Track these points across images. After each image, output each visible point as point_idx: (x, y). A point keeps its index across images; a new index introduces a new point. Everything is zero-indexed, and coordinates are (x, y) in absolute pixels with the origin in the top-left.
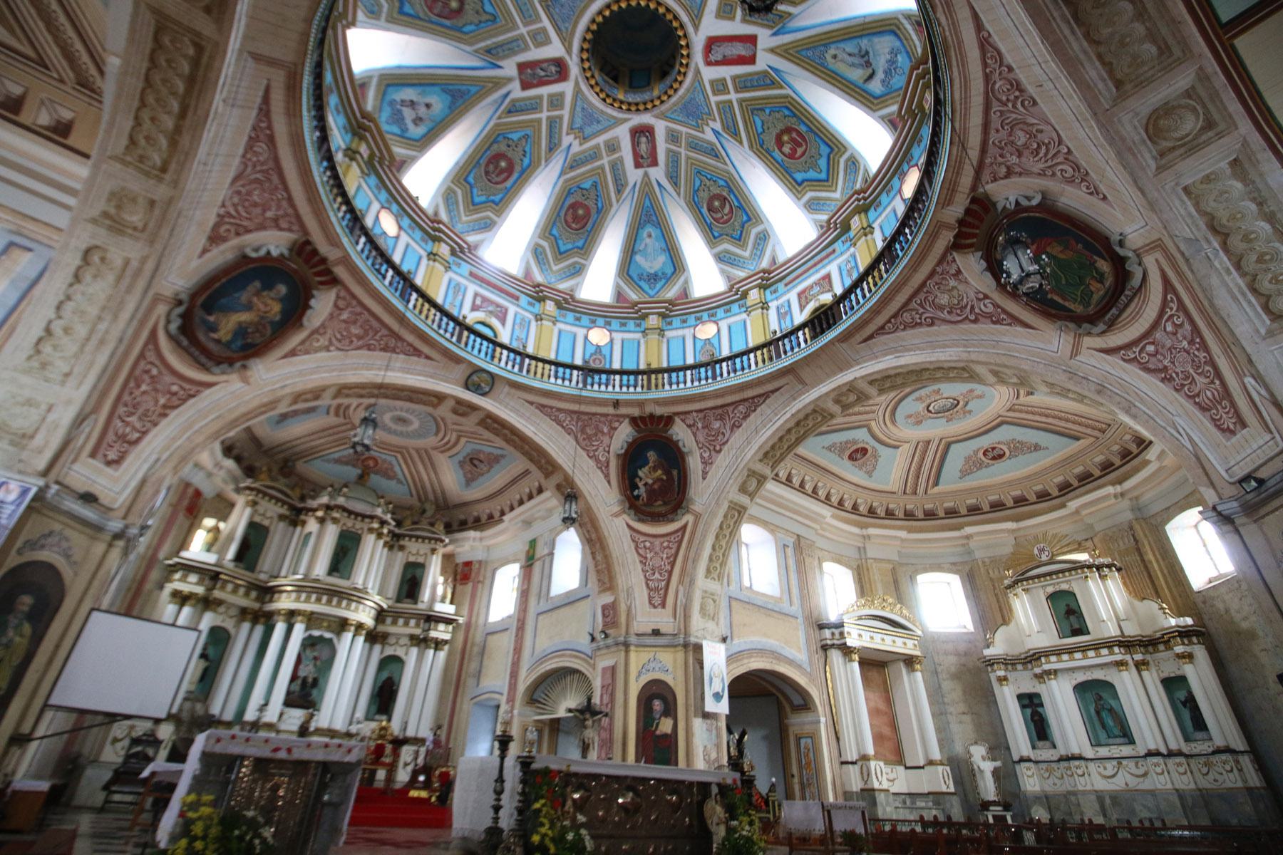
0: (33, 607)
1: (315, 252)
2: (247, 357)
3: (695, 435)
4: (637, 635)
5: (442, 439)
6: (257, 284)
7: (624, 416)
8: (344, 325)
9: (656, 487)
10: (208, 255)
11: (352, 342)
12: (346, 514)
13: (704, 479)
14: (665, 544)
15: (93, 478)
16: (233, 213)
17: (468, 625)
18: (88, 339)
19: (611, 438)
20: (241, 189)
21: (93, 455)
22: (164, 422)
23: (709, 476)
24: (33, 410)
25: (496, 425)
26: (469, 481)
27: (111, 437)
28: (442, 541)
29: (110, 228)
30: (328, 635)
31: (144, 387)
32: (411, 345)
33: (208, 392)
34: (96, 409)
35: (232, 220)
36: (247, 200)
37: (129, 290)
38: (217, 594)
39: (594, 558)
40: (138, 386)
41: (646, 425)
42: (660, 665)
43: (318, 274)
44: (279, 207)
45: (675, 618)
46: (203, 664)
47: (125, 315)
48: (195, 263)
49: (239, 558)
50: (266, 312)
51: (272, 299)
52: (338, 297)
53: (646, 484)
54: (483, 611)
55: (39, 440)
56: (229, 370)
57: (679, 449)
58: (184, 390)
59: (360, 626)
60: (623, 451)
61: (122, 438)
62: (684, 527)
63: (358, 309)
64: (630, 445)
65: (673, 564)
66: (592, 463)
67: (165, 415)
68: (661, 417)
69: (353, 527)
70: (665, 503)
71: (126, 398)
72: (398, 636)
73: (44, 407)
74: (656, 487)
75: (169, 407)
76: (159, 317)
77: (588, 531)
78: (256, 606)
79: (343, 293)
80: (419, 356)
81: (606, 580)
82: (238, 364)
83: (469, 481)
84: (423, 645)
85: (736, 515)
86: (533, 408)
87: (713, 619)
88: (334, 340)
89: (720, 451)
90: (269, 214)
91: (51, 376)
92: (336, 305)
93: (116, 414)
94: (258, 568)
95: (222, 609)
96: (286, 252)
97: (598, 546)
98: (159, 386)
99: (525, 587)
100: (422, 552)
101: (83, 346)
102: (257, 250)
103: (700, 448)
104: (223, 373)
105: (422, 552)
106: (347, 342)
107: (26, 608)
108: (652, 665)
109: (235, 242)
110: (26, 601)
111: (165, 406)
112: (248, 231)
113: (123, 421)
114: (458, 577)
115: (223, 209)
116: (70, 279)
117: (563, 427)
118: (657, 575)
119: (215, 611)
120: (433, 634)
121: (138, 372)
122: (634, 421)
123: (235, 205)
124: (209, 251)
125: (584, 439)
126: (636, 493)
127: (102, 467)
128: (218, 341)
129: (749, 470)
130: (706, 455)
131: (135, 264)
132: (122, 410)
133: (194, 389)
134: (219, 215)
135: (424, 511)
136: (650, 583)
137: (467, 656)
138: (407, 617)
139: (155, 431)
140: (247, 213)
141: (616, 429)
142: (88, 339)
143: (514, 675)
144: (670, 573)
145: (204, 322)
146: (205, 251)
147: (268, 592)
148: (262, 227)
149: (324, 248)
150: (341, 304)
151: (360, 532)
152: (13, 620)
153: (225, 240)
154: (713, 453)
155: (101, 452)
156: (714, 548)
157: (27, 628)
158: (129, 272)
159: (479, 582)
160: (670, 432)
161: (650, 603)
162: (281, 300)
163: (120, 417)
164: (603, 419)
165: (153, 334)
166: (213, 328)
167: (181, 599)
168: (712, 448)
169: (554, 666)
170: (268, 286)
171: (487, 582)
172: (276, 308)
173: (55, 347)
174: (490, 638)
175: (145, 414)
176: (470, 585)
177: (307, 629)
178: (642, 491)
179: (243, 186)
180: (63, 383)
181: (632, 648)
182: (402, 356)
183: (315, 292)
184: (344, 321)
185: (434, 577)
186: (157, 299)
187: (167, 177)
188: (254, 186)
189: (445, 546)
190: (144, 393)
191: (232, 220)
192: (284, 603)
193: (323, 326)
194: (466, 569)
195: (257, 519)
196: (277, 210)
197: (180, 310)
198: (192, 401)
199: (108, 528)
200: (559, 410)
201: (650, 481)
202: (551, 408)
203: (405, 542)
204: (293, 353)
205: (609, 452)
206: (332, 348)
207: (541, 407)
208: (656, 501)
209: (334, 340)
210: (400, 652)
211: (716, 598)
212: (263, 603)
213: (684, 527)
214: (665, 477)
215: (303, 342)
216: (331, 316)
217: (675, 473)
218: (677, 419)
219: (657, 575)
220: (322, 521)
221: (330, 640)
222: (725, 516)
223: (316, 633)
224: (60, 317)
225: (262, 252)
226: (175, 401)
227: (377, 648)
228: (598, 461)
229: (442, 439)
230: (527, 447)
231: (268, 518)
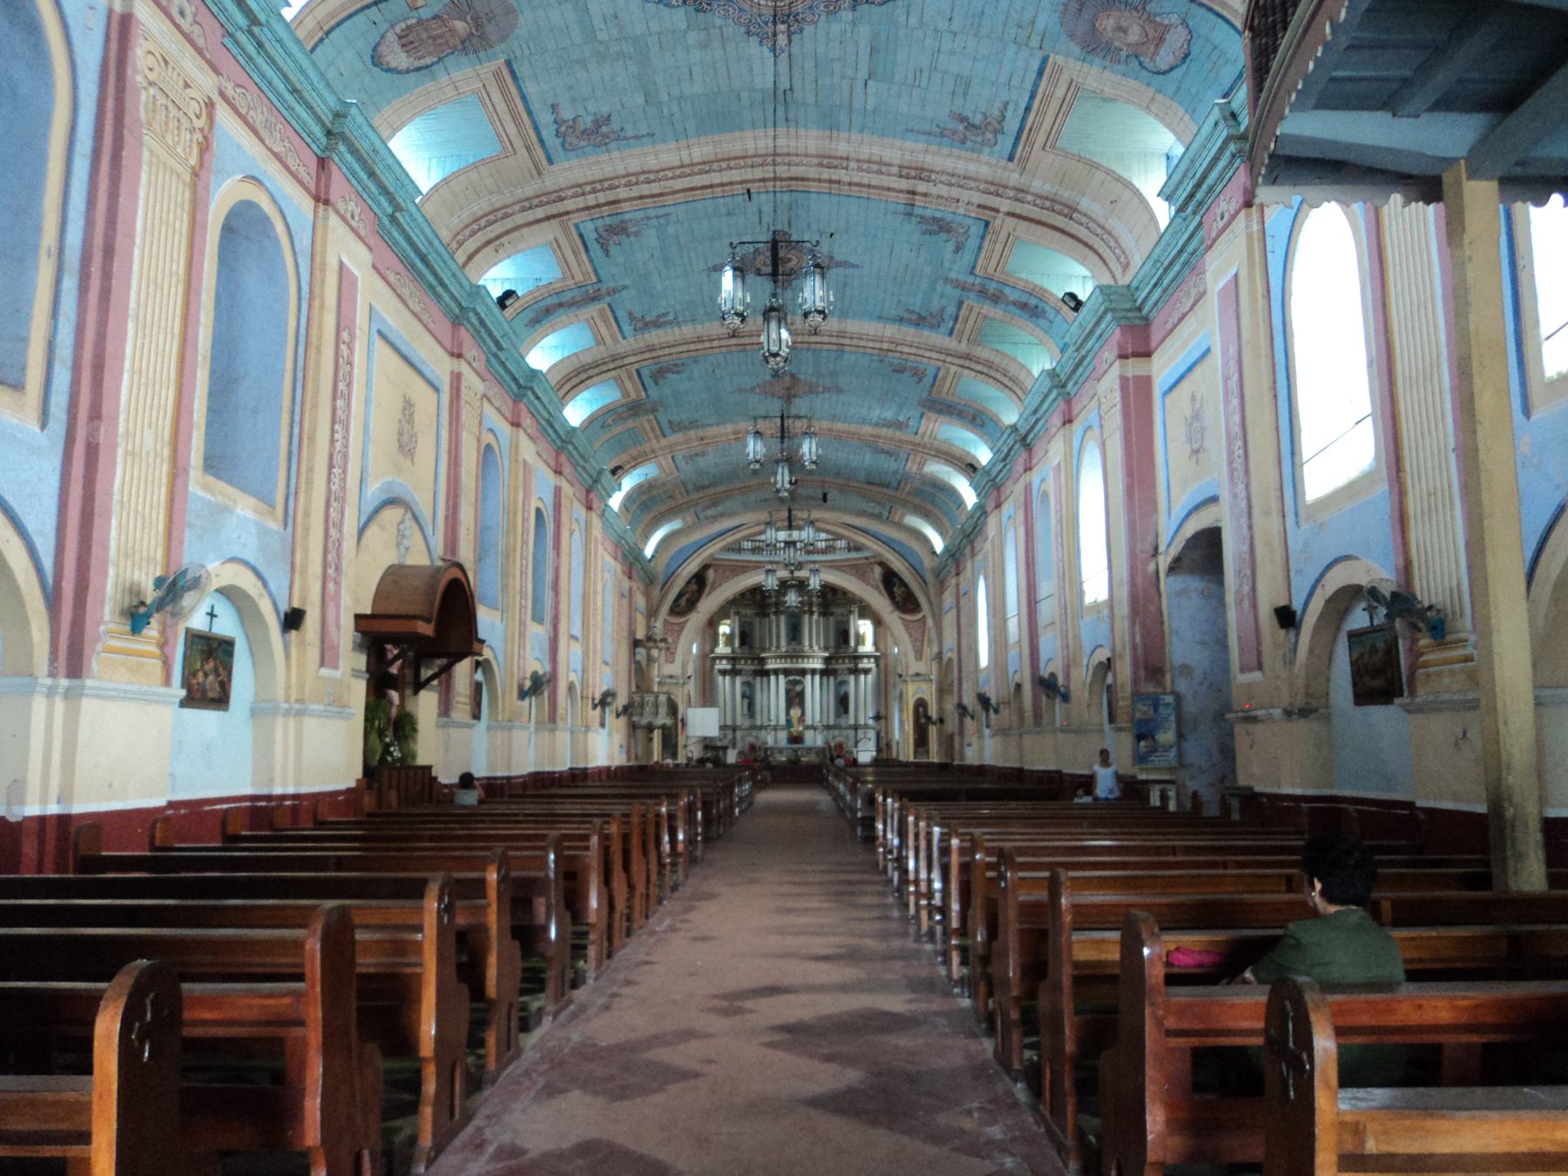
30: (798, 678)
38: (738, 667)
46: (746, 701)
49: (743, 642)
59: (813, 672)
66: (869, 588)
78: (759, 668)
120: (861, 666)
138: (844, 658)
147: (762, 661)
167: (724, 673)
178: (898, 599)
192: (771, 666)
210: (845, 678)
220: (776, 613)
223: (792, 678)
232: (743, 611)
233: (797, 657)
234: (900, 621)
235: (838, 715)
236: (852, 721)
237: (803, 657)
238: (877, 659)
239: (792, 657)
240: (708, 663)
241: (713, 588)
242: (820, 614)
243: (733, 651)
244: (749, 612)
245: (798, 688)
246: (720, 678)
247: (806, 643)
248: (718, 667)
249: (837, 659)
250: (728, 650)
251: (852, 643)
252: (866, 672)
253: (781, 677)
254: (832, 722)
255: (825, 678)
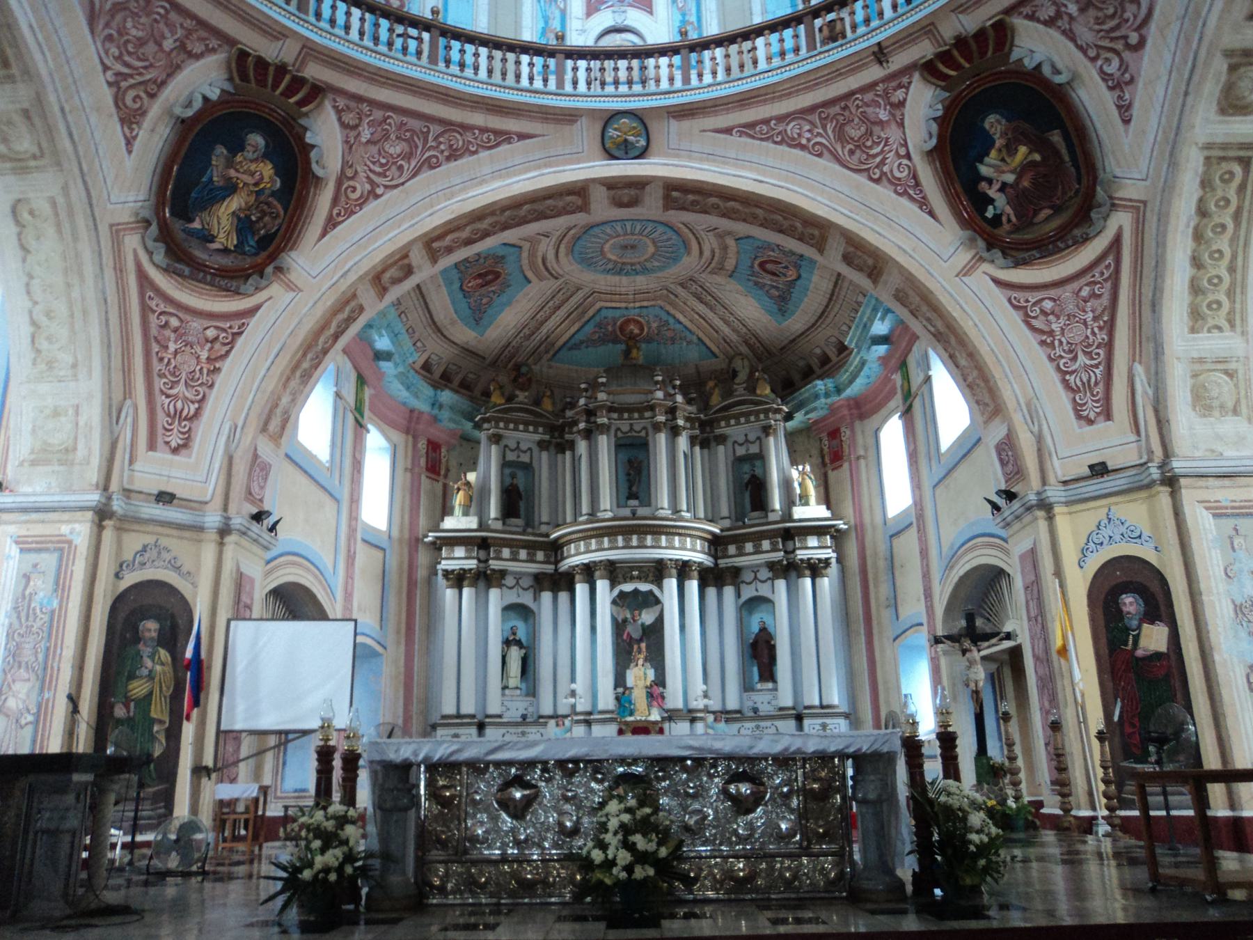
0: (161, 632)
1: (261, 63)
2: (272, 258)
3: (1070, 35)
4: (1065, 483)
5: (701, 253)
6: (220, 150)
7: (908, 70)
8: (374, 149)
9: (1026, 183)
10: (137, 144)
11: (401, 168)
12: (615, 415)
13: (1127, 122)
14: (1085, 292)
15: (166, 473)
16: (126, 70)
17: (859, 528)
18: (72, 316)
19: (901, 125)
20: (107, 31)
21: (152, 446)
22: (220, 379)
23: (1135, 111)
24: (63, 419)
25: (691, 197)
26: (782, 301)
27: (162, 419)
28: (778, 411)
29: (15, 171)
30: (644, 587)
31: (172, 347)
32: (484, 130)
33: (253, 321)
34: (128, 392)
35: (132, 81)
36: (128, 41)
37: (75, 238)
38: (495, 564)
39: (957, 367)
40: (167, 347)
41: (958, 67)
42: (1123, 529)
43: (290, 92)
44: (171, 27)
45: (1138, 433)
46: (515, 654)
47: (89, 269)
48: (129, 163)
50: (256, 184)
51: (255, 160)
52: (339, 112)
53: (1004, 187)
54: (877, 502)
55: (81, 452)
56: (264, 282)
57: (1046, 83)
58: (224, 330)
59: (683, 570)
60: (934, 141)
61: (177, 415)
62: (1117, 242)
63: (378, 114)
64: (941, 121)
65: (1110, 327)
66: (884, 192)
67: (217, 370)
68: (981, 34)
69: (631, 429)
70: (1057, 210)
71: (157, 366)
72: (755, 569)
73: (71, 412)
74: (1026, 183)
75: (215, 361)
76: (135, 251)
77: (928, 320)
78: (549, 568)
79: (341, 103)
80: (509, 140)
81: (987, 400)
82: (269, 269)
83: (782, 301)
84: (793, 574)
85: (1237, 169)
86: (734, 139)
87: (1235, 412)
88: (372, 176)
89: (1142, 43)
90: (168, 44)
91: (62, 373)
92: (344, 125)
93: (157, 392)
94: (536, 523)
95: (509, 581)
96: (228, 87)
97: (953, 340)
98: (191, 339)
99: (912, 447)
100: (752, 437)
101: (72, 325)
102: (189, 104)
103: (1093, 60)
104: (258, 289)
105: (752, 437)
106: (394, 171)
107: (154, 634)
108: (1106, 532)
109: (155, 109)
110: (150, 627)
111: (208, 358)
112: (163, 84)
113: (168, 396)
114: (827, 460)
115: (109, 73)
116: (20, 253)
117: (803, 147)
118: (1082, 359)
119: (500, 586)
120: (801, 554)
121: (154, 331)
122: (929, 69)
123: (119, 58)
124: (135, 138)
125: (852, 152)
126: (990, 213)
127: (170, 457)
128: (225, 251)
129: (1229, 54)
130: (1113, 68)
131: (61, 200)
132: (159, 383)
133: (236, 324)
134: (110, 84)
135: (735, 374)
136: (1071, 378)
137: (871, 576)
138: (757, 538)
139: (213, 395)
140: (139, 59)
141: (902, 104)
142: (72, 316)
143: (928, 594)
144: (1109, 346)
145: (192, 233)
146: (129, 143)
147: (555, 549)
148: (173, 70)
149: (270, 51)
150: (349, 118)
151: (643, 434)
152: (145, 650)
153: (142, 112)
154: (1127, 55)
155: (160, 440)
156: (1196, 262)
157: (164, 654)
158: (63, 215)
159: (858, 458)
160: (1015, 56)
161: (1079, 417)
162: (266, 156)
163: (162, 392)
164: (869, 97)
165: (142, 277)
166: (206, 237)
167: (458, 579)
168: (1119, 46)
169: (968, 567)
170: (237, 147)
171: (872, 452)
172: (267, 170)
173: (49, 339)
174: (896, 541)
175: (191, 377)
176: (846, 465)
177: (612, 586)
179: (107, 25)
180: (75, 377)
181: (1057, 509)
182: (484, 154)
183: (303, 122)
184: (369, 142)
185: (781, 470)
186: (117, 232)
187: (15, 70)
188: (119, 17)
189: (789, 417)
190: (176, 353)
191: (132, 81)
192: (576, 557)
193: (346, 164)
194: (835, 442)
195: (511, 457)
196: (173, 33)
197: (154, 229)
198: (240, 341)
199: (206, 525)
200: (781, 119)
201: (1010, 178)
202: (766, 122)
203: (722, 429)
204: (331, 223)
205: (908, 156)
206: (379, 191)
207: (748, 129)
208: (1036, 213)
209: (372, 176)
210: (764, 590)
211: (1232, 366)
212: (557, 563)
213: (1117, 242)
214: (1037, 157)
215: (335, 201)
216: (349, 145)
217: (1056, 137)
218: (1018, 22)
219: (1082, 359)
220: (588, 434)
221: (651, 592)
222: (1206, 184)
223: (628, 587)
224: (36, 303)
225: (198, 104)
226: (220, 349)
227: (729, 591)
228: (894, 182)
229: (701, 253)
230: (759, 212)
231: (525, 452)
232: (514, 436)
233: (642, 531)
234: (1000, 295)
235: (747, 687)
236: (786, 699)
237: (657, 531)
238: (838, 537)
239: (627, 531)
240: (423, 558)
241: (344, 208)
242: (693, 441)
243: (482, 526)
244: (528, 438)
245: (647, 617)
246: (450, 594)
247: (664, 501)
248: (445, 565)
249: (739, 540)
250: (471, 522)
251: (777, 503)
252: (816, 569)
253: (602, 585)
254: (732, 704)
255: (711, 592)
